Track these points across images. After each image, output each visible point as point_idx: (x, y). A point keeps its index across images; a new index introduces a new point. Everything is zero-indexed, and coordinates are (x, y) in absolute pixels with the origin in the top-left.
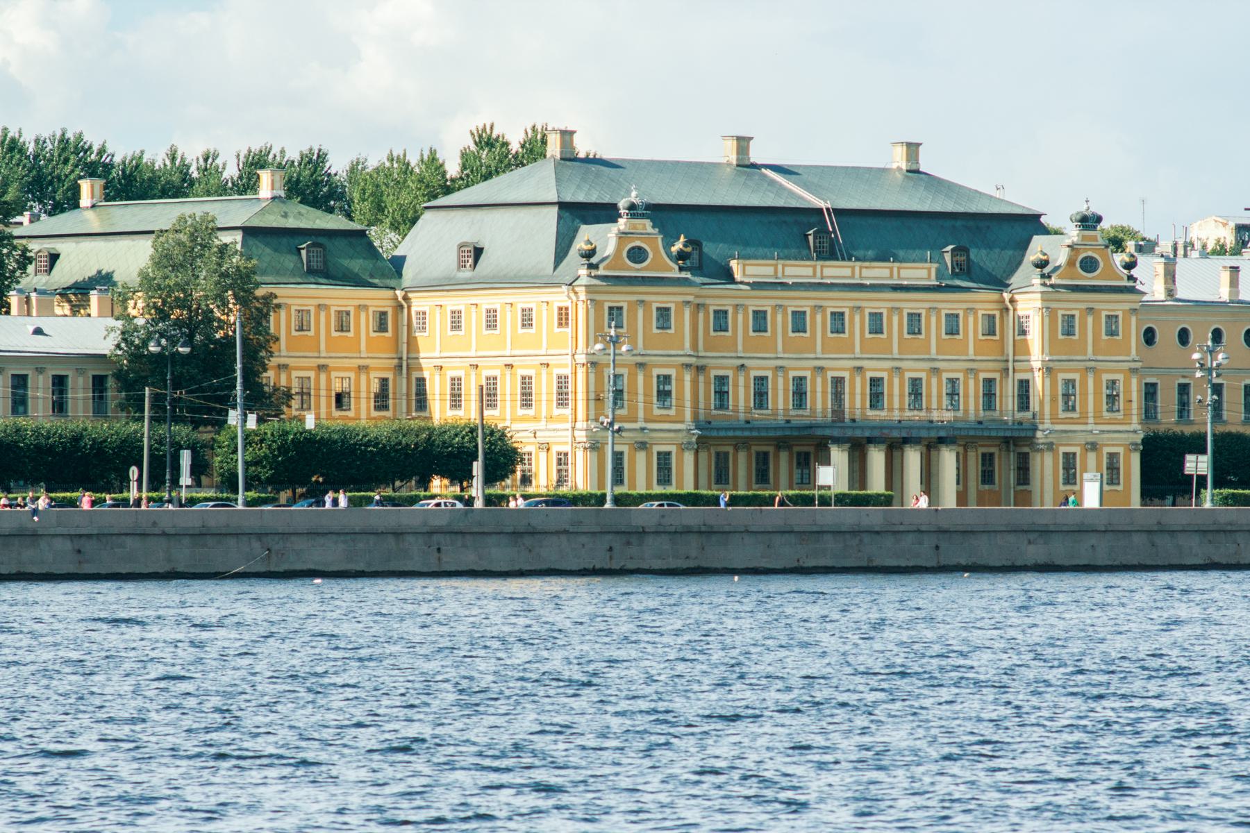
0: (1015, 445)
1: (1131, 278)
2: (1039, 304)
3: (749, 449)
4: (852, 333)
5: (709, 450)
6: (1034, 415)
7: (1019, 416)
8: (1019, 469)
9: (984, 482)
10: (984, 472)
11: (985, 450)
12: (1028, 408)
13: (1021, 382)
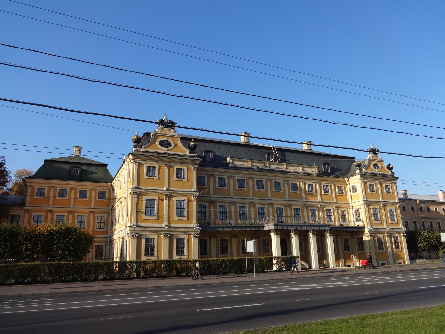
1: (392, 172)
6: (363, 222)
7: (357, 224)
8: (359, 244)
9: (345, 250)
10: (345, 246)
11: (345, 237)
12: (360, 220)
13: (356, 210)
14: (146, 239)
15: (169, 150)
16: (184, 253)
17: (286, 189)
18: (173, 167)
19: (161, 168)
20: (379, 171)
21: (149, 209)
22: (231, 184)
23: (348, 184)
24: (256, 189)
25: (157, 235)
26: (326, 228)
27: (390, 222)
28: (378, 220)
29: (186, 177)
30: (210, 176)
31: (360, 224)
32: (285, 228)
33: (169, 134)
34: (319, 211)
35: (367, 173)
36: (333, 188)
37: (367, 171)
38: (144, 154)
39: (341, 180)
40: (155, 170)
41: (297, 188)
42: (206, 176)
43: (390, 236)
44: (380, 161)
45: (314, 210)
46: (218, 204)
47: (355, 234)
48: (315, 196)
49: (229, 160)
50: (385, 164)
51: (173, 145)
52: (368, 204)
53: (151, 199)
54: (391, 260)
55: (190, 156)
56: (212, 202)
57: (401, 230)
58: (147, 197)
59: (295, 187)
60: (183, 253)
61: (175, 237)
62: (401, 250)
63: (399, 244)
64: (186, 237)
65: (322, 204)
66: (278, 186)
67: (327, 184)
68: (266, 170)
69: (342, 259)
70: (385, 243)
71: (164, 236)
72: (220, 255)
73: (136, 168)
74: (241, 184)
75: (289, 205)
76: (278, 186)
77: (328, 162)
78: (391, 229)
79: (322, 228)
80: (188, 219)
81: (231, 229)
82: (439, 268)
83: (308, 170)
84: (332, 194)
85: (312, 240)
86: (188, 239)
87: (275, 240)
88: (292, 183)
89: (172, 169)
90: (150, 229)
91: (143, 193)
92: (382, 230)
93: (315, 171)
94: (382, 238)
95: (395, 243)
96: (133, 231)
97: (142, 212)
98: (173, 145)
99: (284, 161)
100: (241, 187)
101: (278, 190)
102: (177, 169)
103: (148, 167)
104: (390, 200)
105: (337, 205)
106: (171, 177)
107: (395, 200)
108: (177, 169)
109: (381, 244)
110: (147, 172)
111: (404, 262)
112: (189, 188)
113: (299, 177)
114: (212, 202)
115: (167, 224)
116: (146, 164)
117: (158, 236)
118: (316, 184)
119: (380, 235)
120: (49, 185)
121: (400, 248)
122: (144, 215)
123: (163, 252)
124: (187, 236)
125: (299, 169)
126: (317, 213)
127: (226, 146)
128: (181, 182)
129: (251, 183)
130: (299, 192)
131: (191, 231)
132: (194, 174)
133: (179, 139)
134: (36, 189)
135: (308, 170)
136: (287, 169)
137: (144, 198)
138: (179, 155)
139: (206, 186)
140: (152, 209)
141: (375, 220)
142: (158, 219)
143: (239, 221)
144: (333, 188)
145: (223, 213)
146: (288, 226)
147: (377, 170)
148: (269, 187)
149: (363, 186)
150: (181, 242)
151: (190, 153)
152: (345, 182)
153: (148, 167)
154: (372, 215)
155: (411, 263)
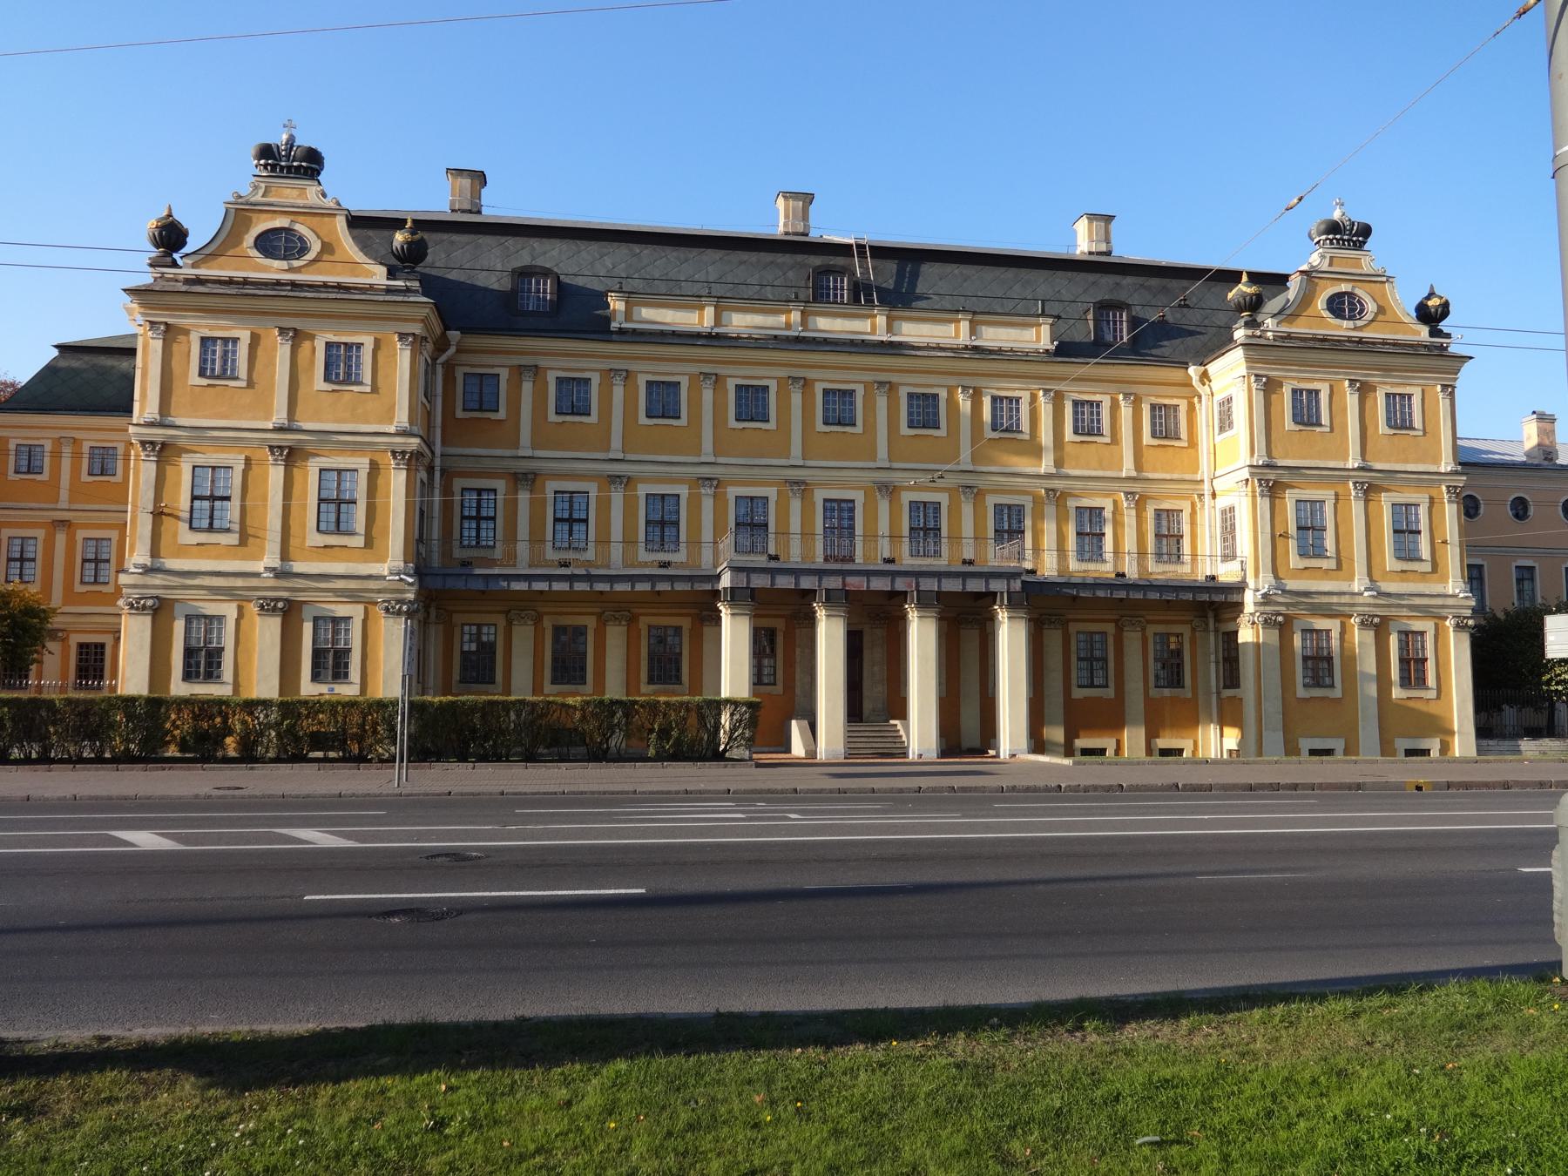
0: (1217, 620)
2: (1242, 369)
3: (632, 620)
4: (870, 427)
5: (538, 621)
11: (1161, 629)
12: (1234, 557)
13: (1224, 512)
14: (189, 619)
15: (298, 270)
16: (346, 675)
17: (881, 418)
18: (312, 337)
19: (264, 343)
20: (1356, 328)
21: (206, 504)
22: (617, 406)
23: (1204, 390)
24: (733, 423)
25: (234, 605)
26: (997, 586)
27: (1391, 563)
28: (1319, 553)
29: (367, 379)
30: (519, 371)
31: (1227, 573)
32: (785, 582)
33: (300, 202)
34: (1038, 516)
35: (1289, 337)
36: (1126, 412)
37: (1285, 328)
38: (184, 288)
39: (1174, 374)
40: (234, 352)
41: (936, 414)
42: (504, 374)
43: (1380, 628)
44: (1378, 279)
45: (1016, 512)
46: (551, 486)
47: (1211, 614)
48: (1035, 450)
49: (616, 304)
50: (1404, 300)
51: (316, 247)
52: (1271, 481)
53: (214, 468)
54: (1368, 733)
55: (389, 291)
56: (526, 479)
57: (1450, 602)
58: (199, 459)
59: (925, 411)
60: (340, 674)
61: (308, 613)
62: (1432, 694)
63: (1430, 666)
64: (356, 612)
65: (1057, 484)
66: (839, 407)
67: (1097, 398)
68: (787, 339)
69: (1135, 723)
70: (1349, 660)
71: (262, 607)
72: (548, 687)
73: (157, 345)
74: (663, 399)
75: (890, 490)
76: (839, 407)
77: (1122, 296)
78: (1381, 594)
79: (975, 586)
80: (369, 543)
81: (564, 586)
82: (1449, 785)
83: (995, 336)
84: (1115, 439)
85: (921, 637)
86: (365, 622)
87: (734, 636)
88: (911, 396)
89: (306, 345)
90: (207, 581)
91: (181, 443)
92: (1335, 599)
93: (1039, 337)
94: (1335, 634)
95: (1404, 661)
96: (134, 586)
97: (178, 518)
98: (316, 247)
99: (899, 299)
100: (663, 417)
101: (839, 424)
102: (329, 345)
103: (204, 340)
104: (1406, 461)
105: (1137, 487)
106: (302, 378)
107: (1437, 461)
108: (329, 345)
109: (1320, 665)
110: (203, 361)
111: (1445, 748)
112: (380, 422)
113: (949, 365)
114: (526, 479)
115: (276, 563)
116: (200, 326)
117: (240, 609)
118: (1034, 398)
119: (1321, 623)
120: (56, 434)
121: (1431, 680)
122: (183, 527)
123: (257, 669)
124: (361, 608)
125: (957, 333)
126: (1028, 523)
127: (636, 248)
128: (347, 396)
129: (708, 395)
130: (942, 432)
131: (379, 591)
132: (402, 361)
133: (340, 223)
134: (12, 446)
135: (995, 336)
136: (889, 329)
137: (185, 466)
138: (339, 287)
139: (502, 414)
140: (217, 503)
141: (1303, 554)
142: (243, 541)
143: (643, 556)
144: (1126, 412)
145: (571, 521)
146: (797, 573)
147: (1345, 323)
148: (795, 414)
149: (1258, 398)
150: (336, 632)
151: (391, 274)
152: (1188, 384)
153: (204, 340)
154: (1292, 529)
155: (1479, 752)
